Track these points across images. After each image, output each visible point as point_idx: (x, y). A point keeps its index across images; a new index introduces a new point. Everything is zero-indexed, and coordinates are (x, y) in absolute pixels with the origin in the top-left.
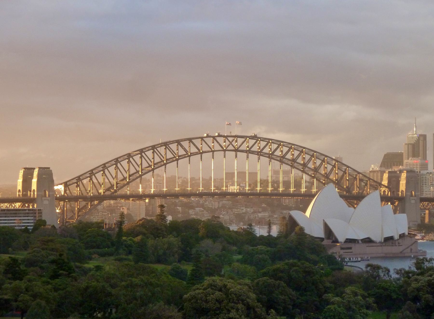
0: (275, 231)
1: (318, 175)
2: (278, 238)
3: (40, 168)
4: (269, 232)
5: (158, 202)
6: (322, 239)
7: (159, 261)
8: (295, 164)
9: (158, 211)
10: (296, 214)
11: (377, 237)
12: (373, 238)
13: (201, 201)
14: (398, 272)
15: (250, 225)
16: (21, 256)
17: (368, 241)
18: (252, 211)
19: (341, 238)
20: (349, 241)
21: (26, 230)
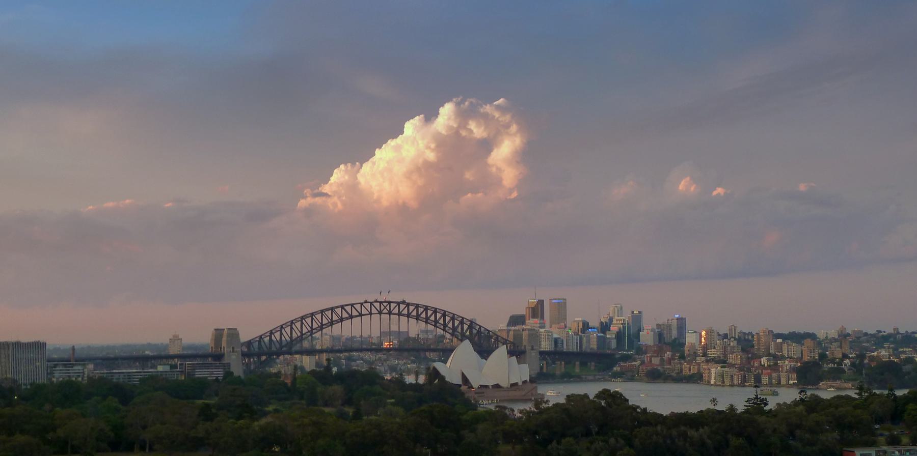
0: (422, 379)
1: (456, 333)
2: (423, 385)
3: (229, 329)
4: (417, 380)
5: (324, 356)
6: (460, 386)
7: (326, 405)
8: (438, 325)
9: (325, 363)
10: (439, 366)
11: (505, 384)
12: (501, 384)
13: (361, 355)
14: (521, 412)
15: (401, 375)
16: (212, 401)
17: (497, 386)
18: (403, 363)
19: (475, 385)
20: (482, 386)
21: (217, 380)
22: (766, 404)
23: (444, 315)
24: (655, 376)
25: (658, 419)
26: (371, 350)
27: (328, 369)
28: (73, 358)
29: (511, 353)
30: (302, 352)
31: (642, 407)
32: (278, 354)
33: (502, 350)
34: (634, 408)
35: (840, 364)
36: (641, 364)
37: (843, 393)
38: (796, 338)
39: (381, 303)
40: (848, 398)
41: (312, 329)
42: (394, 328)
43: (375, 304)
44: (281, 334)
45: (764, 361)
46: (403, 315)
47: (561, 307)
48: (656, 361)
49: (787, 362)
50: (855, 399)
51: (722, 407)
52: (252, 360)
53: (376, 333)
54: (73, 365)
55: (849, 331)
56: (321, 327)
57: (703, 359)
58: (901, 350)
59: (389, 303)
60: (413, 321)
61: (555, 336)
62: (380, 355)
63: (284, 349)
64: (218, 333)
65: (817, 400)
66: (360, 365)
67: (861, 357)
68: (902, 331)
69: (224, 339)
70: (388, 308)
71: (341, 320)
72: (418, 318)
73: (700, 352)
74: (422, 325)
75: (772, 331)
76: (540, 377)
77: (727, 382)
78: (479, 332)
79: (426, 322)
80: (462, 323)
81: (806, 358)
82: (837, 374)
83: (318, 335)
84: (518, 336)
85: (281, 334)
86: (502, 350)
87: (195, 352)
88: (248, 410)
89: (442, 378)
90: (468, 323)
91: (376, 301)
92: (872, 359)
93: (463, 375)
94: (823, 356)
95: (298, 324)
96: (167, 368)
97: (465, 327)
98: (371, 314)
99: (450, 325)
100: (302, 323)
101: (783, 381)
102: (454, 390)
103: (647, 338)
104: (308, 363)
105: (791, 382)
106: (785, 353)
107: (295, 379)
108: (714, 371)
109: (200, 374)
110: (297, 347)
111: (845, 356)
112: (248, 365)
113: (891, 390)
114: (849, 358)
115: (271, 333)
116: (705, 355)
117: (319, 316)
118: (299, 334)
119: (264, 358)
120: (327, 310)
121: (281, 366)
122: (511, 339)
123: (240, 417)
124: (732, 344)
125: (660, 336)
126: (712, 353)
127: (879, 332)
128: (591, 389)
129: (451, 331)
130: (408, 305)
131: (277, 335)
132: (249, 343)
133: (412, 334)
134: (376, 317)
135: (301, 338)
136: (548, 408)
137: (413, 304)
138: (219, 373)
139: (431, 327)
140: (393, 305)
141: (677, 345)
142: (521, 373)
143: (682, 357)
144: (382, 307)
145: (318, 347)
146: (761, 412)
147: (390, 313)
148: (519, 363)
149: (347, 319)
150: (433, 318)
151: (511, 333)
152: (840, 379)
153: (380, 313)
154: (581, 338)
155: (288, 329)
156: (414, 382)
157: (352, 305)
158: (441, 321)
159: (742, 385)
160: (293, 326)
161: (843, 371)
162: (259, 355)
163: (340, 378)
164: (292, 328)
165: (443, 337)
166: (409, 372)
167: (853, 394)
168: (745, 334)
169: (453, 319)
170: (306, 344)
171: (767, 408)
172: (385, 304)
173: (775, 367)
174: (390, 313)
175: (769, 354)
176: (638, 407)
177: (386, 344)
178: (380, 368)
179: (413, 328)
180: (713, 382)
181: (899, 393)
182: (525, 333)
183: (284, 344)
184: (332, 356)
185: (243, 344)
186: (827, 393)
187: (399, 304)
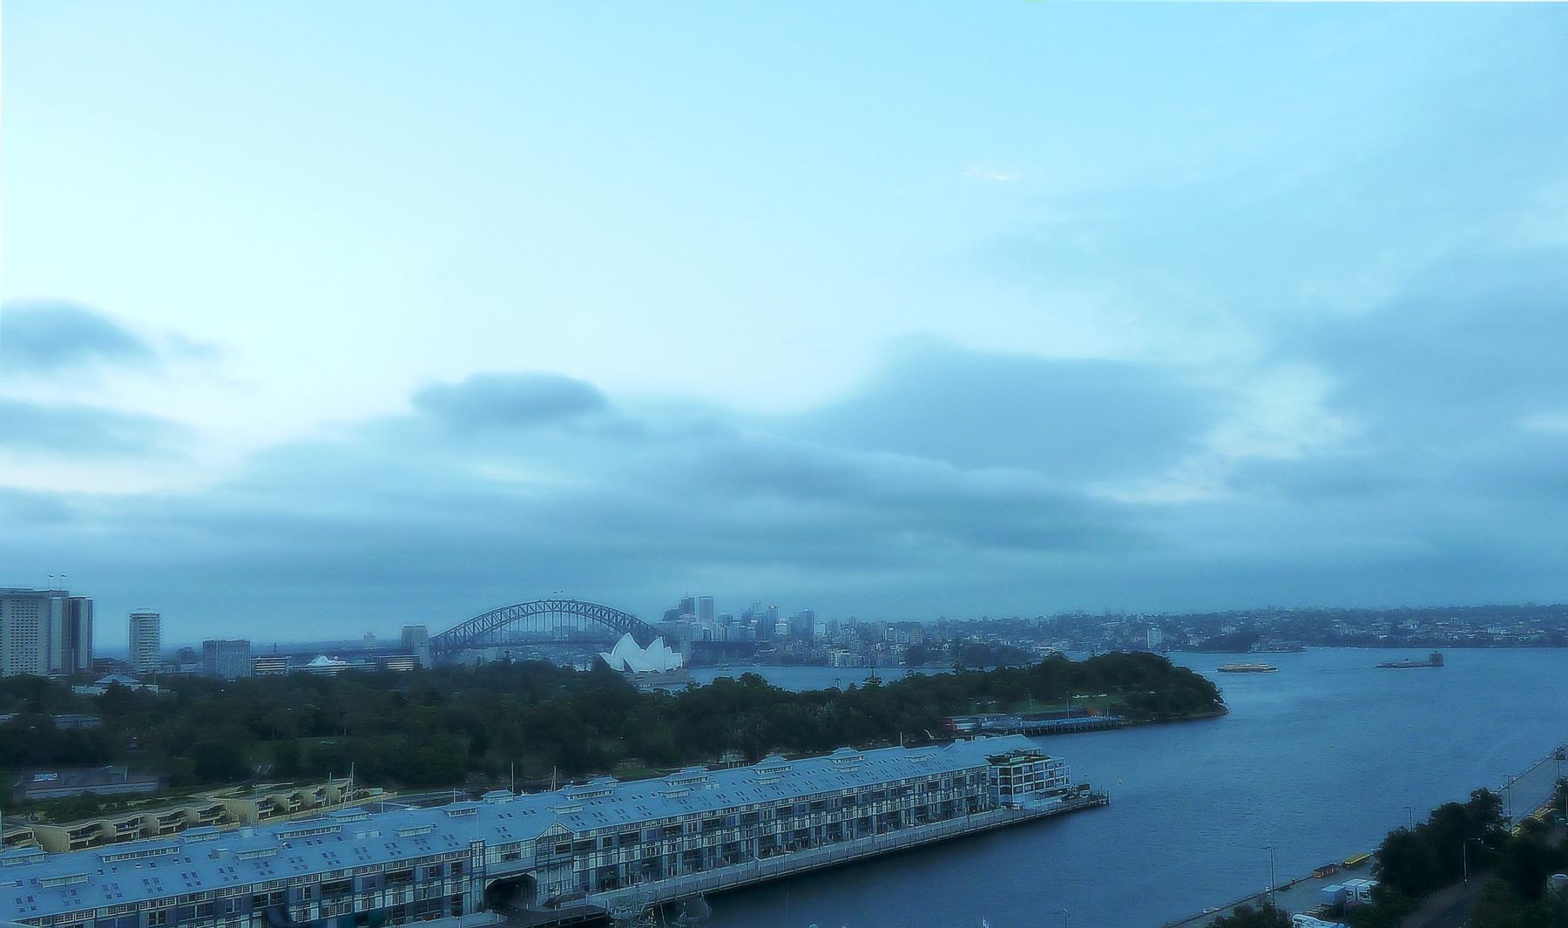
5: (505, 649)
14: (678, 693)
17: (655, 672)
23: (609, 612)
24: (788, 661)
27: (507, 660)
44: (465, 631)
46: (574, 612)
66: (535, 655)
67: (957, 641)
80: (624, 618)
85: (465, 631)
92: (966, 642)
93: (625, 661)
94: (926, 641)
97: (627, 622)
98: (544, 611)
103: (782, 628)
108: (838, 655)
114: (947, 643)
121: (467, 658)
125: (792, 628)
126: (836, 640)
128: (735, 673)
130: (577, 603)
132: (435, 639)
141: (807, 635)
142: (675, 660)
149: (523, 616)
161: (942, 653)
179: (581, 624)
181: (989, 669)
185: (430, 640)
186: (929, 672)
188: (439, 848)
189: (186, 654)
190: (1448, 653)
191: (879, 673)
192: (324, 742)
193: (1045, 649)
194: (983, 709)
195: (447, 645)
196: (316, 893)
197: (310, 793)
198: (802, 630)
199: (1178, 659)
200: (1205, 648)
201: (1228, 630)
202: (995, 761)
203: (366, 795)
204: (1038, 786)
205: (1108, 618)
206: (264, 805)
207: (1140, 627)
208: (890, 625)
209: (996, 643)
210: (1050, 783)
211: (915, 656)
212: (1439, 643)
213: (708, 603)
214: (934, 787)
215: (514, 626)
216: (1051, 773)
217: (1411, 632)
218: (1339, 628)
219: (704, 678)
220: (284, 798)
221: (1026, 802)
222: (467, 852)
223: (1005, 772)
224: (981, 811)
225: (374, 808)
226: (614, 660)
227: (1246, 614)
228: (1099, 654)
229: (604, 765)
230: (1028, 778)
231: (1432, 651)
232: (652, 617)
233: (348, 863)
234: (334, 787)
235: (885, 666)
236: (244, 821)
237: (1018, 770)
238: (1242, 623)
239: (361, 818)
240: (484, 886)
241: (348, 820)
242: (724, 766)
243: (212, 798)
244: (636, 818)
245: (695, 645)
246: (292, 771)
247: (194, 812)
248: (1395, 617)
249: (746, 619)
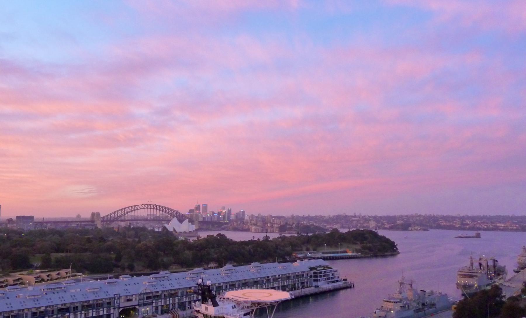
0: (160, 230)
3: (97, 213)
5: (129, 222)
7: (129, 238)
9: (129, 224)
10: (166, 226)
11: (187, 231)
15: (154, 228)
16: (91, 236)
17: (185, 232)
21: (92, 230)
22: (269, 238)
23: (168, 209)
24: (235, 229)
25: (235, 243)
26: (144, 220)
27: (130, 226)
28: (43, 222)
29: (189, 222)
30: (122, 221)
31: (231, 239)
32: (113, 221)
33: (187, 221)
34: (228, 239)
35: (292, 226)
36: (231, 225)
37: (293, 235)
38: (279, 218)
39: (148, 205)
40: (294, 236)
41: (125, 213)
42: (152, 213)
43: (146, 205)
44: (114, 215)
45: (269, 225)
47: (205, 208)
48: (235, 224)
49: (276, 225)
50: (296, 237)
51: (256, 239)
52: (104, 223)
53: (146, 215)
54: (43, 224)
55: (295, 215)
56: (128, 213)
57: (250, 224)
58: (310, 221)
59: (150, 205)
60: (158, 211)
61: (204, 216)
62: (147, 222)
63: (115, 219)
64: (93, 214)
65: (284, 237)
66: (140, 225)
67: (298, 224)
68: (311, 216)
69: (95, 216)
70: (150, 206)
71: (134, 210)
72: (159, 210)
73: (249, 222)
74: (161, 212)
75: (271, 216)
76: (199, 230)
77: (257, 231)
78: (179, 215)
79: (162, 211)
80: (174, 212)
81: (282, 224)
82: (291, 229)
83: (126, 215)
84: (192, 216)
85: (114, 215)
86: (187, 221)
87: (85, 220)
88: (102, 239)
89: (167, 230)
90: (176, 212)
91: (146, 204)
92: (301, 224)
94: (286, 223)
95: (120, 211)
96: (76, 225)
97: (175, 213)
99: (170, 212)
100: (121, 211)
101: (274, 231)
102: (171, 233)
104: (123, 224)
105: (277, 231)
106: (275, 222)
107: (118, 229)
108: (254, 227)
109: (87, 227)
110: (120, 219)
111: (293, 223)
112: (103, 225)
113: (307, 234)
115: (111, 214)
116: (250, 223)
117: (127, 209)
118: (120, 215)
119: (108, 222)
120: (130, 207)
121: (114, 225)
122: (190, 217)
123: (100, 242)
124: (259, 219)
126: (253, 222)
127: (304, 216)
128: (215, 233)
129: (170, 214)
130: (156, 206)
131: (113, 215)
132: (103, 217)
133: (158, 215)
134: (146, 209)
135: (121, 216)
136: (201, 239)
137: (158, 206)
138: (93, 227)
139: (164, 213)
140: (151, 206)
141: (242, 220)
142: (193, 228)
143: (244, 223)
144: (148, 206)
145: (127, 219)
146: (268, 241)
147: (150, 208)
148: (192, 225)
150: (164, 210)
151: (190, 215)
152: (292, 230)
153: (147, 208)
154: (212, 217)
155: (117, 213)
156: (158, 230)
157: (138, 205)
158: (167, 211)
159: (262, 232)
160: (118, 212)
161: (292, 228)
162: (107, 221)
163: (134, 228)
164: (118, 213)
165: (168, 216)
166: (156, 227)
167: (296, 235)
168: (263, 216)
169: (171, 210)
170: (123, 218)
171: (269, 239)
172: (149, 205)
173: (272, 227)
174: (150, 208)
175: (270, 223)
176: (230, 239)
177: (149, 219)
178: (147, 226)
179: (158, 213)
180: (253, 231)
181: (310, 235)
182: (194, 215)
183: (115, 218)
184: (131, 222)
185: (102, 217)
187: (153, 205)
188: (102, 296)
189: (10, 221)
190: (481, 232)
191: (268, 235)
192: (60, 255)
193: (330, 227)
194: (308, 250)
195: (108, 220)
196: (55, 312)
197: (54, 274)
198: (240, 217)
199: (381, 233)
200: (391, 228)
201: (399, 222)
202: (311, 269)
203: (76, 276)
204: (328, 279)
205: (355, 216)
206: (37, 278)
207: (366, 220)
208: (273, 217)
209: (313, 225)
210: (332, 278)
211: (282, 229)
212: (480, 229)
213: (205, 208)
214: (288, 278)
215: (133, 213)
216: (333, 274)
217: (468, 224)
218: (441, 223)
219: (203, 235)
220: (44, 276)
221: (324, 285)
222: (113, 298)
223: (315, 273)
224: (306, 288)
225: (78, 281)
226: (170, 227)
227: (407, 216)
228: (351, 230)
229: (166, 267)
230: (324, 276)
231: (476, 232)
232: (184, 211)
233: (68, 299)
234: (63, 272)
235: (271, 232)
236: (29, 284)
237: (320, 273)
238: (405, 219)
239: (74, 284)
240: (119, 311)
241: (68, 284)
242: (211, 268)
243: (17, 275)
244: (177, 287)
245: (200, 222)
246: (47, 265)
247: (10, 280)
248: (462, 219)
249: (219, 214)
